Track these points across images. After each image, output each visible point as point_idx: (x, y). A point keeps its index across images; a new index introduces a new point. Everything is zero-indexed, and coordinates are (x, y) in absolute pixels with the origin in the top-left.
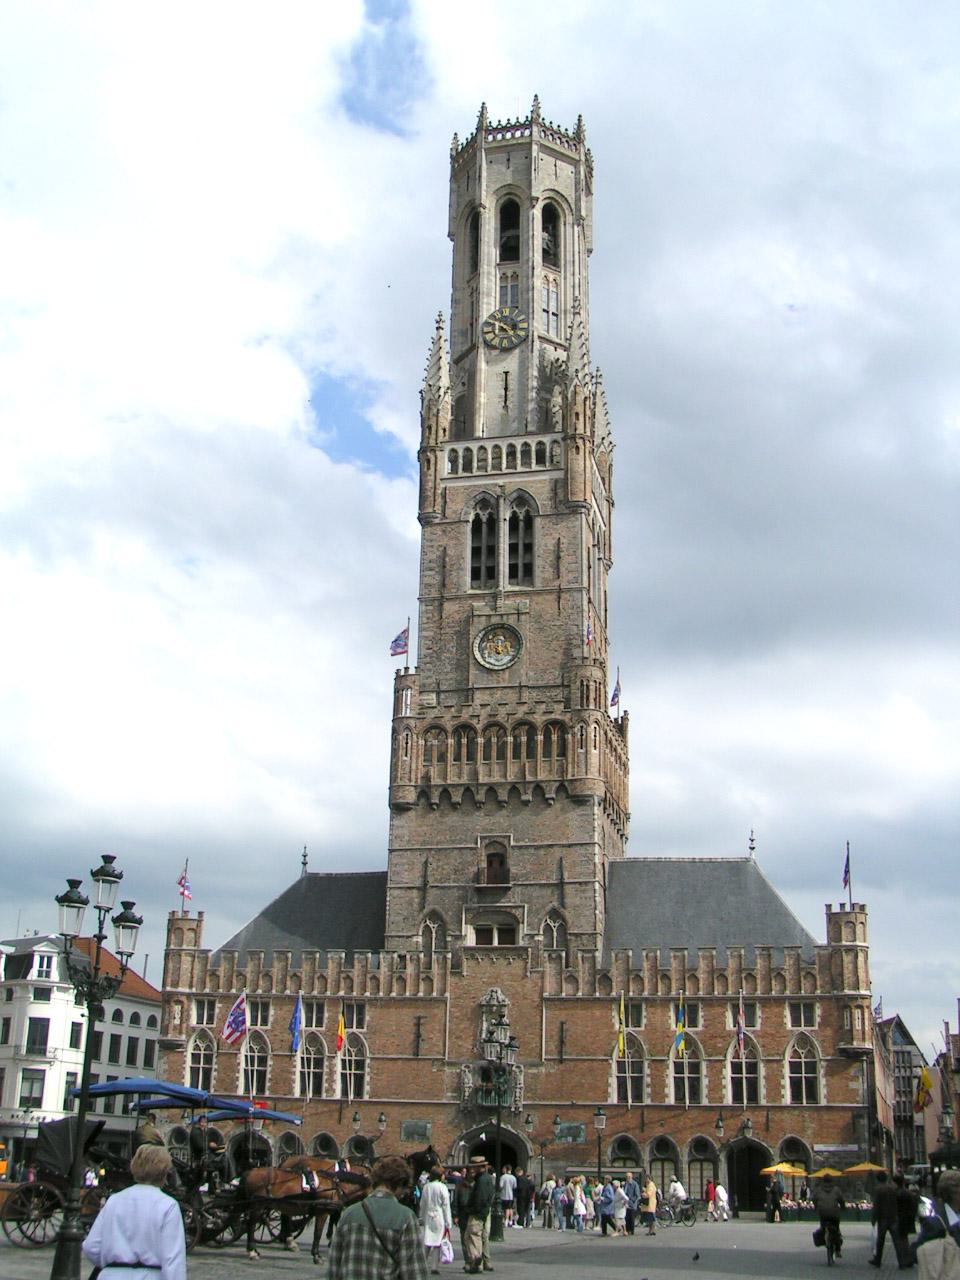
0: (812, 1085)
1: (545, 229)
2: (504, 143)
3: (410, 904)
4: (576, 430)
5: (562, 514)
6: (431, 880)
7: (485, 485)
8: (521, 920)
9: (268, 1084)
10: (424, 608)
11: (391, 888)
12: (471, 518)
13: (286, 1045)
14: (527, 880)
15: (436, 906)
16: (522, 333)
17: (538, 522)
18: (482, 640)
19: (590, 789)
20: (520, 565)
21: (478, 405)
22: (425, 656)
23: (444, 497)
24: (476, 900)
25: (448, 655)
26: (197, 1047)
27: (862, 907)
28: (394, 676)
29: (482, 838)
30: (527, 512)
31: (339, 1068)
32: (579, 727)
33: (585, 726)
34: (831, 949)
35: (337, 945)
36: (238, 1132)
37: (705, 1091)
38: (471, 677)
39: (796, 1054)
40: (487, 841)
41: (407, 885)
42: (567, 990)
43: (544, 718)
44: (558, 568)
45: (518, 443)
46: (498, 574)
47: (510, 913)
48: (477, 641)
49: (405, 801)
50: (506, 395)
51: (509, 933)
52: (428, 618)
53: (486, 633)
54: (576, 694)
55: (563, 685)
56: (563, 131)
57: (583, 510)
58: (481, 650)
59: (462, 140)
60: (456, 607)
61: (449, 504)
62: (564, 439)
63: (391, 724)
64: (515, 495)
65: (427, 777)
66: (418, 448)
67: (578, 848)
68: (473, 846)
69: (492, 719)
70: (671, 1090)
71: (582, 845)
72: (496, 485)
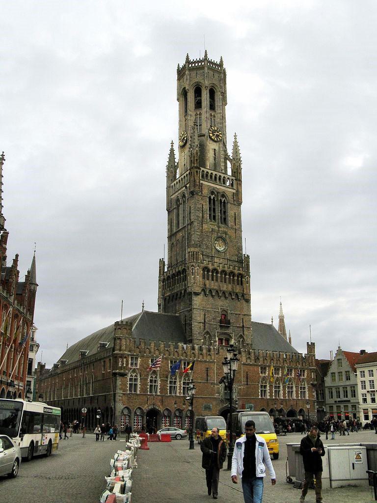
0: (304, 392)
3: (200, 328)
6: (206, 320)
7: (213, 187)
9: (159, 390)
13: (165, 376)
15: (208, 330)
23: (202, 187)
26: (131, 376)
27: (314, 343)
29: (221, 309)
31: (182, 385)
34: (309, 355)
35: (181, 341)
36: (150, 408)
38: (213, 253)
51: (228, 341)
55: (237, 261)
60: (206, 227)
64: (222, 194)
65: (205, 285)
70: (274, 394)
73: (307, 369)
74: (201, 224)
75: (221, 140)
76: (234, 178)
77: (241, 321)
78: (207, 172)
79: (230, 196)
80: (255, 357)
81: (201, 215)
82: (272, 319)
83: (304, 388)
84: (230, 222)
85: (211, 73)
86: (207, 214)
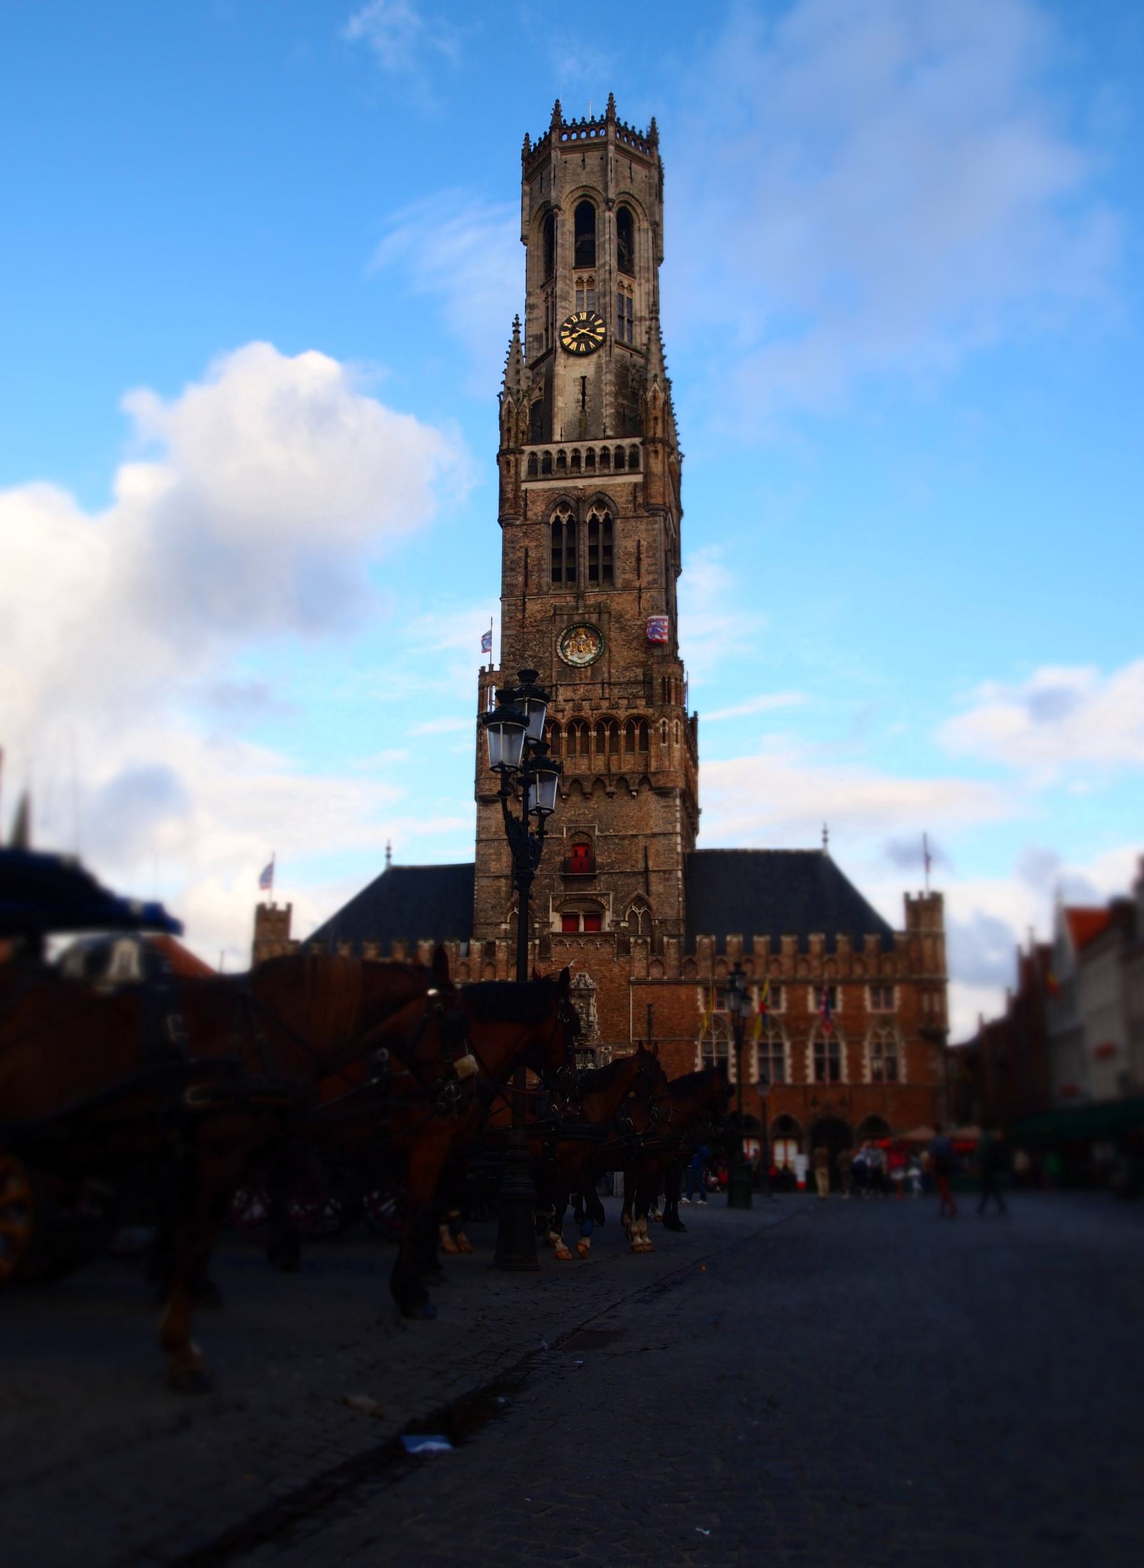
1: (619, 235)
2: (579, 143)
3: (498, 891)
4: (655, 434)
5: (641, 517)
8: (606, 907)
10: (506, 607)
11: (478, 877)
12: (552, 520)
14: (612, 868)
16: (600, 338)
17: (619, 524)
18: (564, 639)
19: (671, 781)
20: (601, 567)
21: (556, 409)
22: (509, 654)
23: (525, 500)
24: (562, 888)
25: (530, 653)
28: (478, 673)
29: (569, 829)
30: (607, 515)
32: (661, 721)
33: (667, 721)
37: (788, 1071)
39: (876, 1035)
40: (573, 831)
41: (494, 875)
42: (656, 973)
43: (627, 713)
44: (638, 569)
45: (597, 445)
46: (579, 575)
47: (596, 902)
48: (560, 640)
49: (492, 793)
50: (584, 400)
51: (594, 918)
52: (511, 618)
53: (568, 632)
54: (658, 690)
55: (644, 682)
56: (637, 132)
57: (662, 513)
58: (562, 650)
59: (534, 140)
60: (538, 607)
61: (530, 506)
62: (642, 443)
63: (476, 719)
64: (594, 498)
66: (497, 451)
67: (661, 838)
68: (561, 836)
69: (576, 714)
71: (665, 834)
72: (576, 488)
73: (901, 982)
74: (519, 603)
75: (600, 345)
76: (637, 441)
77: (640, 856)
78: (547, 453)
79: (622, 500)
80: (680, 959)
81: (521, 579)
82: (825, 832)
83: (891, 1046)
84: (623, 572)
85: (576, 157)
86: (540, 570)
